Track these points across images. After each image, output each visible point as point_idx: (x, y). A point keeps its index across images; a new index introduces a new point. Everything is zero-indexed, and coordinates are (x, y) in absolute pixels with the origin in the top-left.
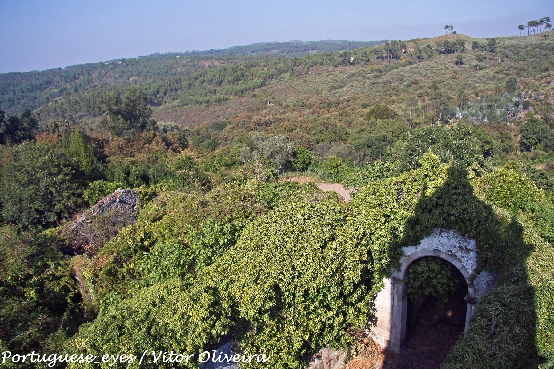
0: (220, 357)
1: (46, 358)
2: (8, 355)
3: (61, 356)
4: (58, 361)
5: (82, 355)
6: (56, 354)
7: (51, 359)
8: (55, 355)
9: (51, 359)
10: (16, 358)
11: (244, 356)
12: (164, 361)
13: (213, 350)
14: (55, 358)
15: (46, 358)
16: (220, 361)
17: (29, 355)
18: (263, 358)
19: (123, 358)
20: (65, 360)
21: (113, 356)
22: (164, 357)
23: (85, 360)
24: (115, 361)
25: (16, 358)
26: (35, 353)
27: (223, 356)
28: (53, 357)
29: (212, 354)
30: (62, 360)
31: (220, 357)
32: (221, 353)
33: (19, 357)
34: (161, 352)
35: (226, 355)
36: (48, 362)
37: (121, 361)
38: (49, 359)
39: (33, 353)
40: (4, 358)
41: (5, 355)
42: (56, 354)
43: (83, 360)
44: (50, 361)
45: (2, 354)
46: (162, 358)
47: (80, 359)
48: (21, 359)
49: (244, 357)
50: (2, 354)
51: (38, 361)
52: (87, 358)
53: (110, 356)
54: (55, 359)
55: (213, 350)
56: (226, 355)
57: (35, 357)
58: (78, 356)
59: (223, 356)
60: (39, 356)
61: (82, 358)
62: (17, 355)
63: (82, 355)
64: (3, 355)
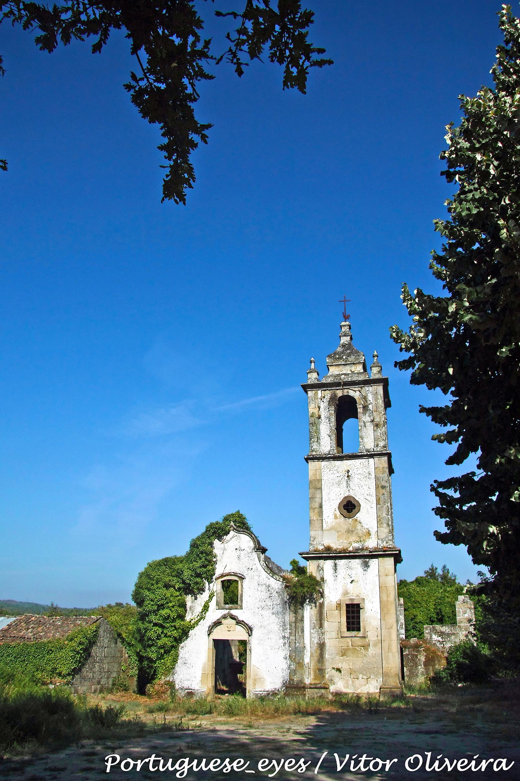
0: (437, 762)
1: (173, 765)
2: (114, 759)
3: (196, 761)
4: (190, 769)
5: (228, 760)
7: (180, 766)
8: (187, 760)
10: (127, 765)
11: (473, 763)
12: (352, 769)
13: (426, 753)
14: (186, 764)
15: (173, 765)
16: (473, 769)
17: (147, 760)
18: (503, 765)
19: (463, 765)
20: (502, 768)
21: (274, 762)
22: (353, 762)
23: (232, 767)
24: (278, 769)
25: (127, 765)
26: (366, 757)
27: (442, 762)
28: (183, 762)
29: (425, 758)
30: (197, 767)
31: (437, 762)
32: (438, 757)
34: (348, 756)
35: (446, 759)
36: (176, 771)
37: (286, 768)
38: (177, 766)
39: (153, 758)
40: (109, 764)
41: (110, 759)
43: (229, 767)
44: (178, 768)
45: (106, 759)
46: (348, 763)
47: (300, 766)
48: (384, 766)
49: (473, 763)
50: (106, 759)
51: (161, 769)
52: (235, 764)
55: (426, 753)
56: (446, 759)
57: (156, 763)
58: (297, 763)
59: (442, 762)
60: (162, 761)
61: (228, 765)
62: (129, 760)
64: (108, 759)
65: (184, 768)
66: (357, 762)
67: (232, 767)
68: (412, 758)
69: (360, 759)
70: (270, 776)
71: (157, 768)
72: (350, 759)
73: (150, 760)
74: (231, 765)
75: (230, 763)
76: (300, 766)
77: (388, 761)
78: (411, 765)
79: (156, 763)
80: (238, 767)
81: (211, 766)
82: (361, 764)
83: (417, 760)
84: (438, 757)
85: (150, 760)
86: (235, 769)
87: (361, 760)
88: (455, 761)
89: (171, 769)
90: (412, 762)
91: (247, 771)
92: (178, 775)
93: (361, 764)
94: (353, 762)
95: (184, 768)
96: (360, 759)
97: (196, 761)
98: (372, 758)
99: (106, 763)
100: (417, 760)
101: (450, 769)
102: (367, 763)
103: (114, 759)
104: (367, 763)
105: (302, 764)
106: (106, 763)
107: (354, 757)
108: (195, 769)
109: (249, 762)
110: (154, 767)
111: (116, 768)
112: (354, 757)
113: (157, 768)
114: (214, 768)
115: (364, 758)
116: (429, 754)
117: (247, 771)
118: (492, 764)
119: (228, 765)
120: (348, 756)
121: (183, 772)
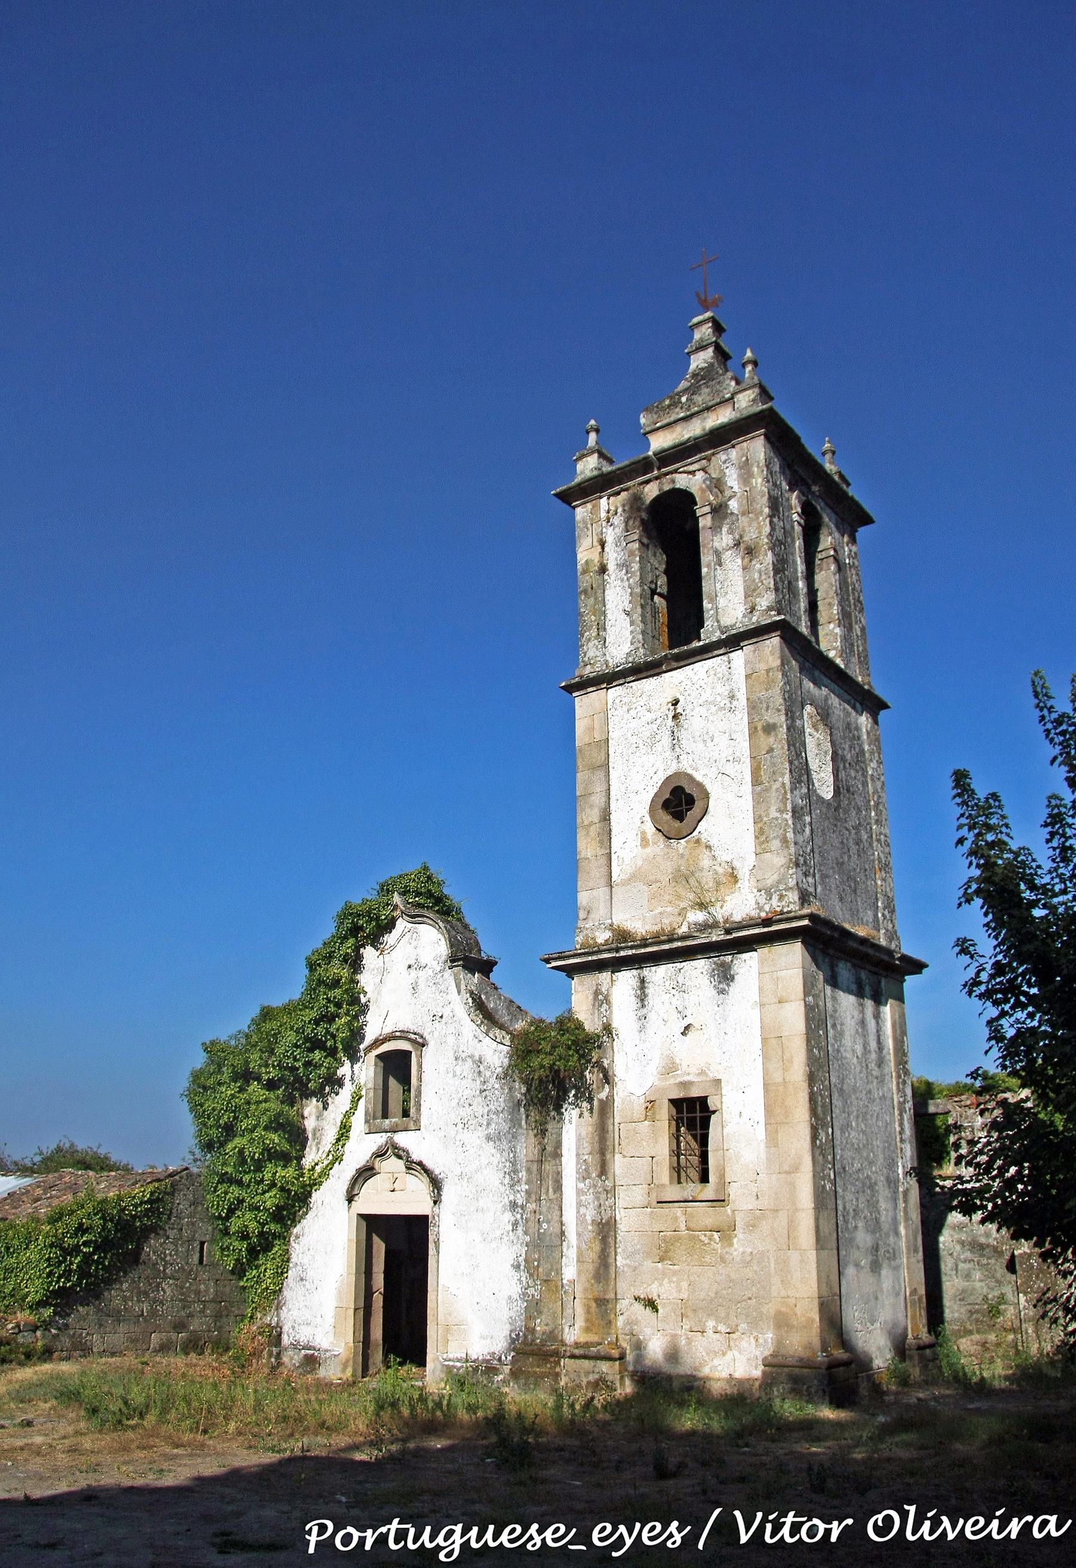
0: (927, 1523)
2: (323, 1529)
3: (475, 1529)
4: (465, 1546)
5: (535, 1527)
6: (460, 1526)
7: (446, 1540)
8: (458, 1528)
9: (446, 1540)
10: (347, 1539)
11: (995, 1523)
12: (768, 1539)
13: (906, 1507)
14: (457, 1536)
15: (432, 1538)
17: (384, 1530)
18: (1051, 1527)
21: (622, 1529)
22: (769, 1526)
23: (544, 1540)
24: (629, 1542)
25: (347, 1539)
27: (936, 1523)
28: (451, 1533)
29: (904, 1516)
30: (478, 1541)
31: (927, 1523)
32: (930, 1515)
33: (356, 1535)
34: (759, 1515)
35: (944, 1518)
36: (439, 1548)
38: (440, 1540)
39: (395, 1525)
40: (313, 1539)
41: (315, 1529)
42: (460, 1526)
43: (538, 1540)
44: (443, 1544)
46: (761, 1528)
49: (995, 1523)
50: (307, 1528)
51: (411, 1546)
52: (548, 1534)
53: (615, 1530)
54: (457, 1539)
55: (906, 1507)
56: (944, 1518)
57: (401, 1535)
59: (936, 1523)
61: (535, 1535)
63: (535, 1527)
64: (311, 1529)
65: (453, 1543)
66: (777, 1527)
67: (544, 1540)
68: (880, 1517)
69: (782, 1520)
70: (614, 1554)
71: (403, 1543)
72: (765, 1520)
73: (389, 1529)
74: (542, 1536)
75: (540, 1532)
76: (671, 1536)
77: (835, 1523)
78: (879, 1531)
79: (401, 1535)
80: (555, 1540)
81: (504, 1538)
82: (786, 1531)
83: (888, 1520)
84: (930, 1515)
85: (389, 1529)
86: (551, 1544)
87: (784, 1523)
88: (961, 1521)
89: (428, 1545)
90: (880, 1523)
91: (570, 1547)
92: (442, 1556)
93: (786, 1531)
94: (769, 1526)
95: (453, 1543)
96: (782, 1520)
97: (475, 1529)
98: (805, 1519)
99: (307, 1537)
100: (888, 1520)
101: (951, 1536)
102: (795, 1528)
103: (323, 1529)
104: (795, 1528)
105: (675, 1533)
106: (307, 1537)
107: (771, 1517)
108: (474, 1545)
109: (574, 1530)
110: (397, 1542)
111: (326, 1546)
112: (771, 1517)
113: (403, 1543)
114: (511, 1541)
115: (790, 1518)
116: (912, 1509)
117: (570, 1547)
118: (1029, 1526)
119: (535, 1535)
120: (759, 1515)
121: (452, 1552)
